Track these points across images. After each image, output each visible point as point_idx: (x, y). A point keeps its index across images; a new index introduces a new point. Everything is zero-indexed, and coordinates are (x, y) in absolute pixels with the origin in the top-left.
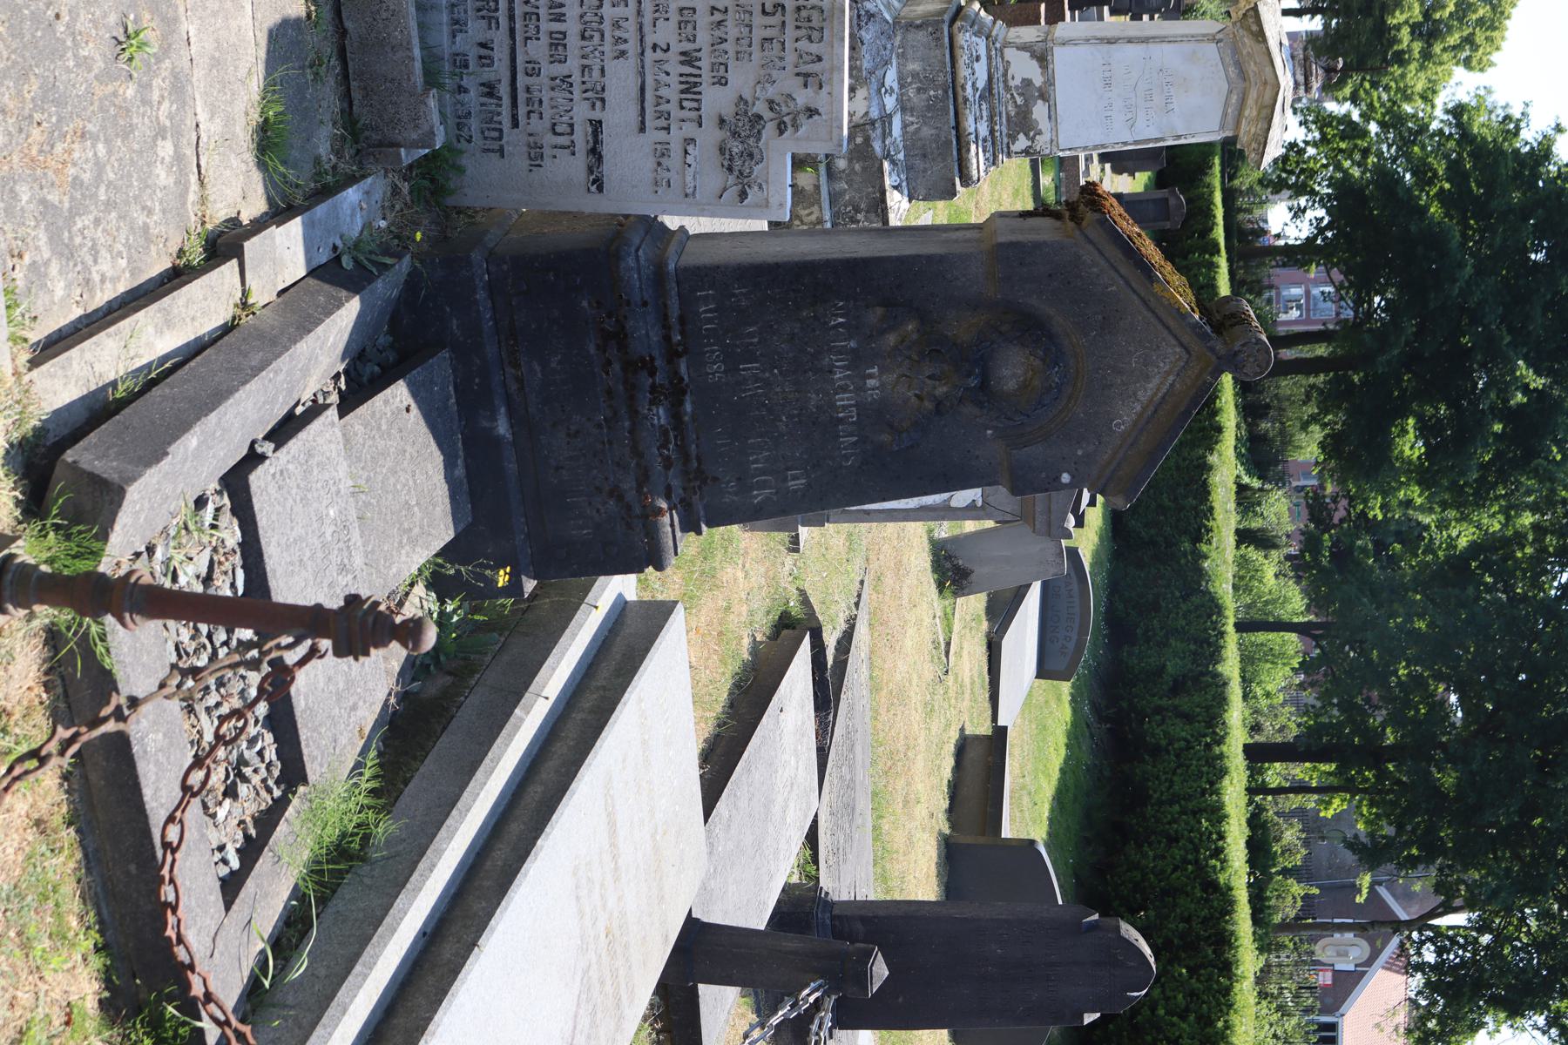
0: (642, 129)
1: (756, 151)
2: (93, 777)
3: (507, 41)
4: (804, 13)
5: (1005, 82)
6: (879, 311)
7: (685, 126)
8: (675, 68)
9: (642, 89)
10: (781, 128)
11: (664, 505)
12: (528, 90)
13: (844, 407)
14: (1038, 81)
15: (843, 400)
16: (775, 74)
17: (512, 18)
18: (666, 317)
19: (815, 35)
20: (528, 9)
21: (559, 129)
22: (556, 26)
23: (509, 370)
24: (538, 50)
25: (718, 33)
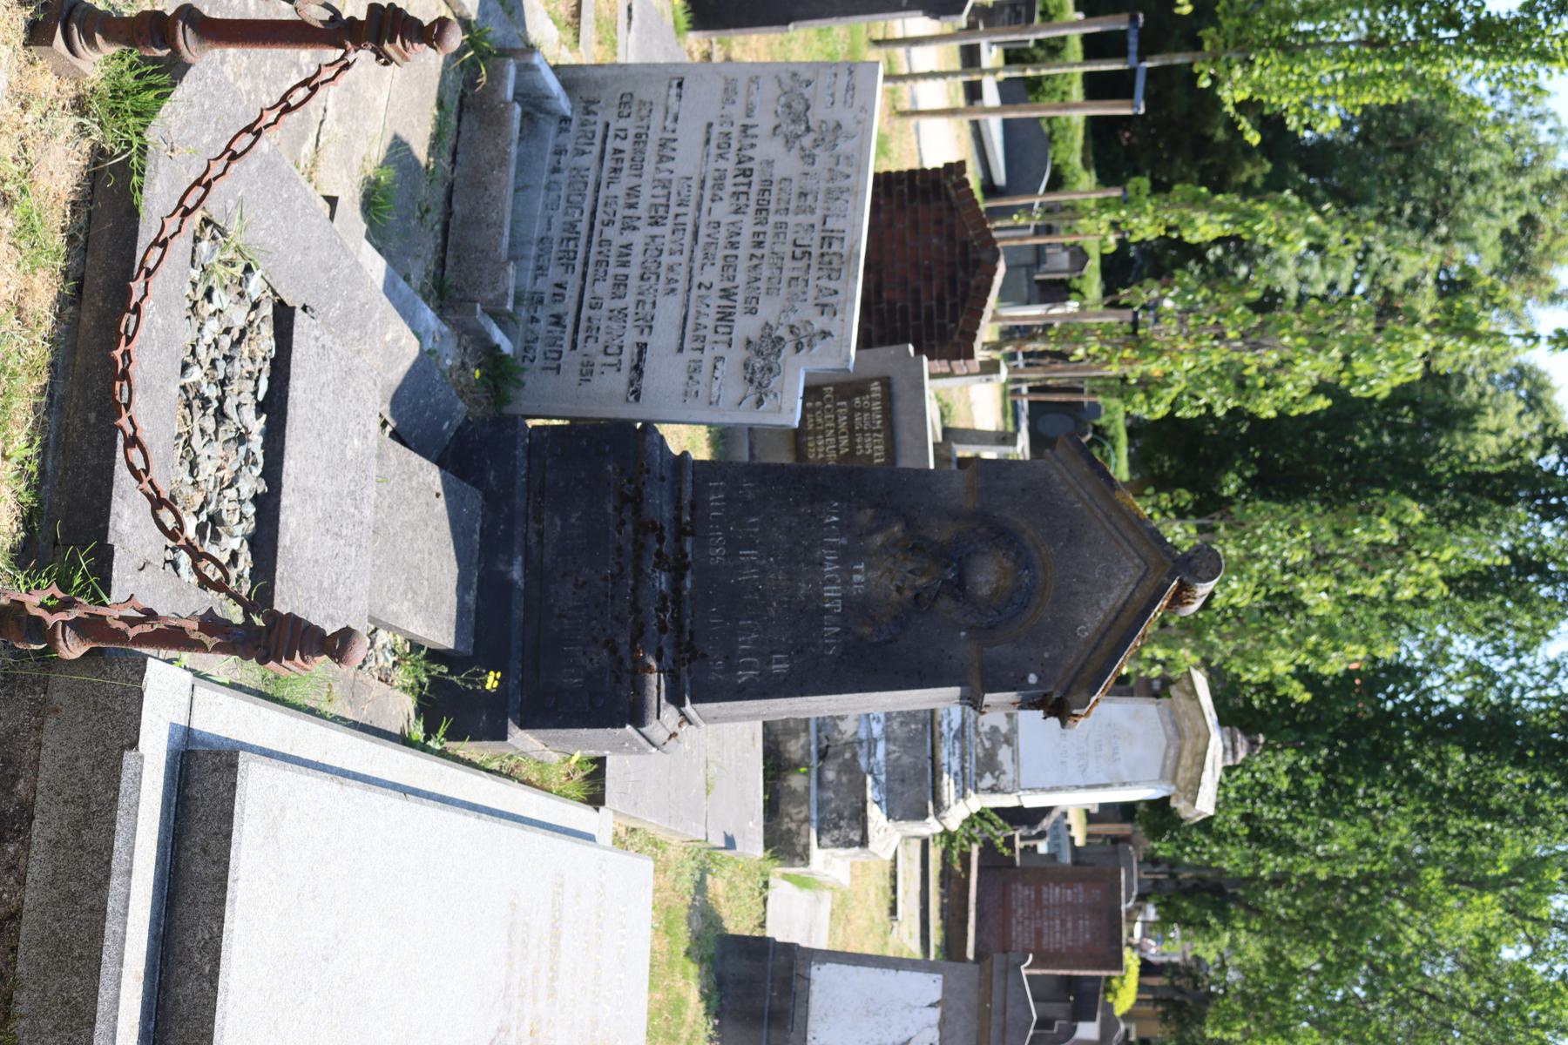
0: (681, 349)
1: (775, 367)
2: (86, 318)
3: (579, 282)
4: (826, 259)
5: (976, 728)
6: (870, 512)
7: (717, 347)
8: (715, 300)
9: (685, 318)
10: (798, 347)
11: (654, 664)
12: (589, 319)
13: (831, 599)
14: (1004, 728)
15: (830, 591)
16: (798, 305)
17: (586, 264)
18: (679, 500)
19: (834, 275)
20: (600, 258)
21: (609, 351)
22: (622, 271)
23: (532, 524)
24: (603, 289)
25: (753, 274)
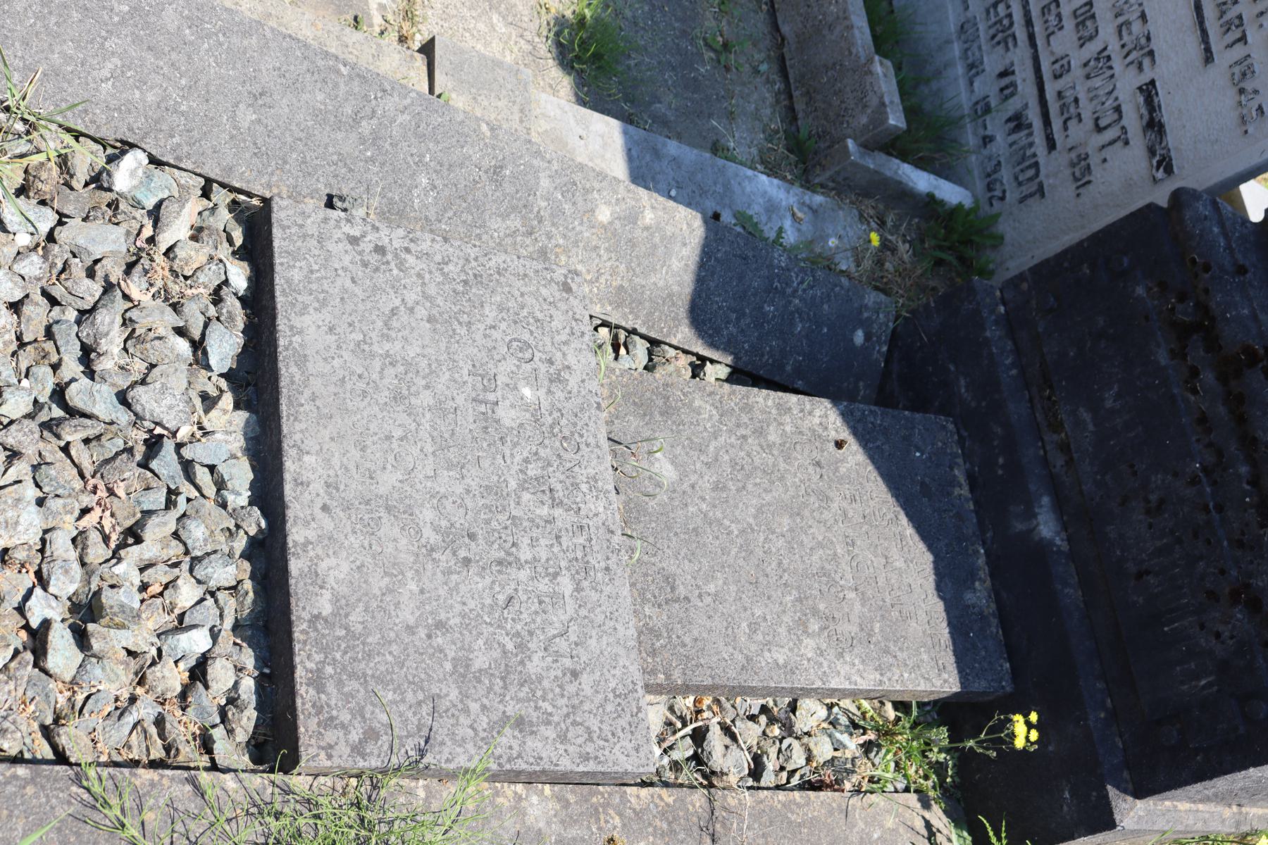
0: (1208, 57)
17: (1029, 23)
21: (1102, 123)
24: (1064, 43)
